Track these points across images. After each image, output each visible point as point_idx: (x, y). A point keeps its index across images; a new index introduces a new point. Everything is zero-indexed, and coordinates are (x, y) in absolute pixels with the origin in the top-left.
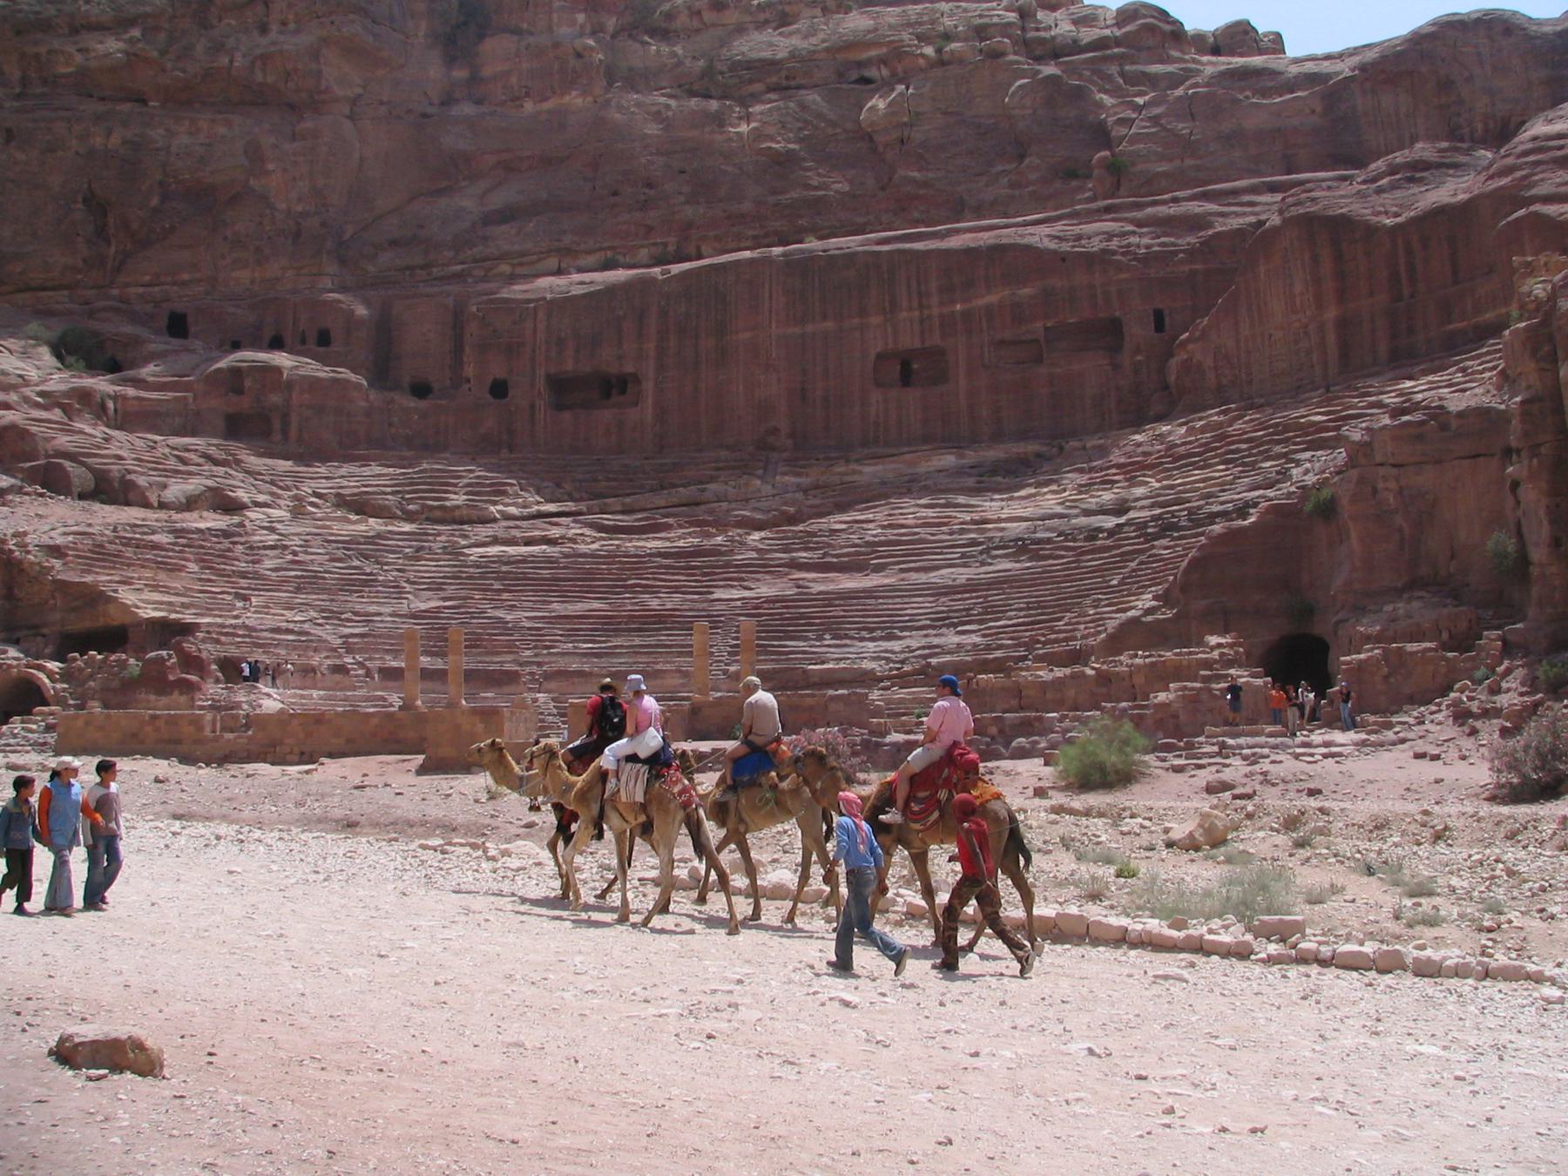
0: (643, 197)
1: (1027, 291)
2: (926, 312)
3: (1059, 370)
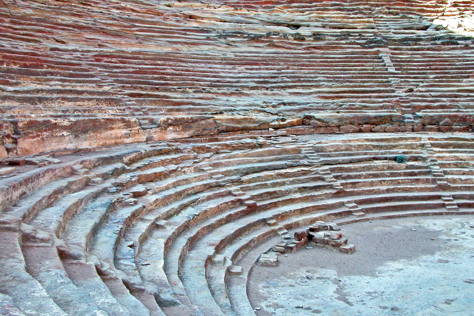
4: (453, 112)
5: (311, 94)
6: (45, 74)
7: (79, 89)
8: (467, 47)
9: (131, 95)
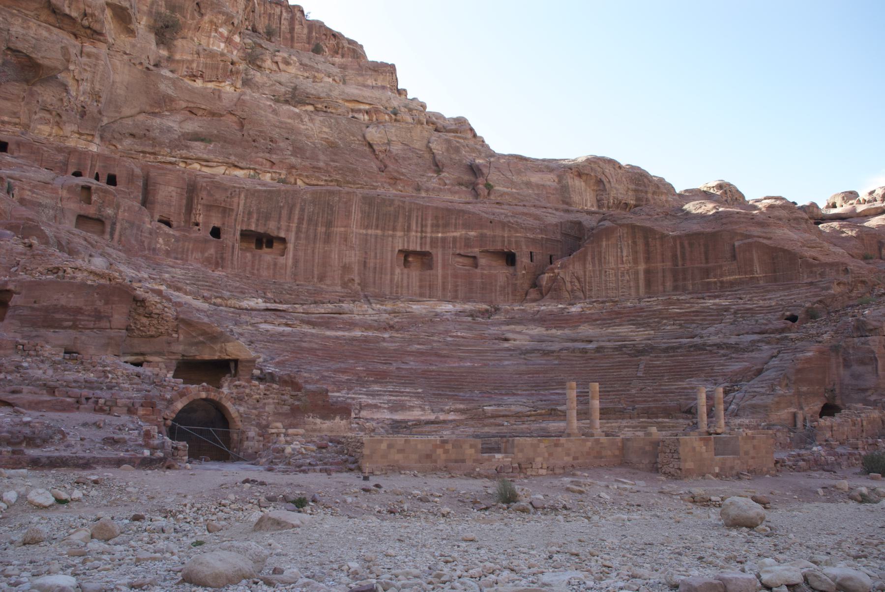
1: (472, 234)
4: (659, 404)
9: (434, 394)
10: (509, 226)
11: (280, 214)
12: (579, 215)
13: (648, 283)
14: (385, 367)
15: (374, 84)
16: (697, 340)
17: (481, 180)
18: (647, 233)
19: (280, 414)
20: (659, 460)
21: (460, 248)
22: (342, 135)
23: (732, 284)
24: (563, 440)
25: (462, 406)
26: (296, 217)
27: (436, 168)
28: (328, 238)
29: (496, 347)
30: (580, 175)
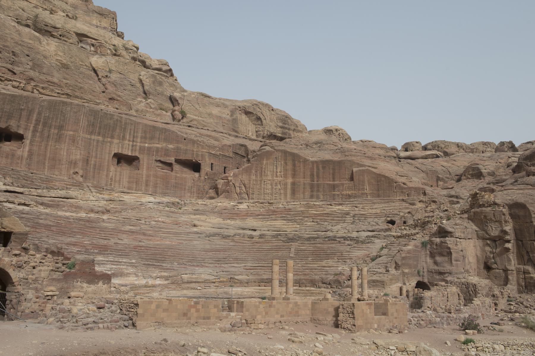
0: (13, 60)
1: (171, 146)
2: (135, 143)
3: (178, 175)
4: (307, 277)
5: (240, 267)
6: (108, 254)
7: (120, 260)
8: (339, 242)
9: (144, 264)
10: (197, 144)
11: (21, 115)
12: (244, 140)
13: (293, 192)
14: (105, 242)
15: (98, 24)
16: (330, 234)
17: (177, 108)
18: (295, 157)
19: (53, 279)
20: (339, 318)
21: (161, 156)
22: (72, 60)
23: (350, 196)
24: (274, 302)
25: (165, 274)
26: (34, 118)
27: (144, 95)
28: (59, 139)
29: (188, 230)
30: (247, 113)
